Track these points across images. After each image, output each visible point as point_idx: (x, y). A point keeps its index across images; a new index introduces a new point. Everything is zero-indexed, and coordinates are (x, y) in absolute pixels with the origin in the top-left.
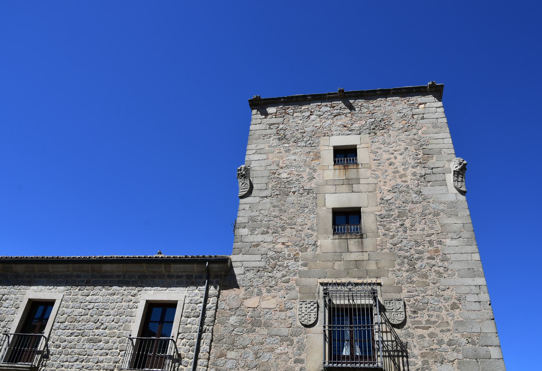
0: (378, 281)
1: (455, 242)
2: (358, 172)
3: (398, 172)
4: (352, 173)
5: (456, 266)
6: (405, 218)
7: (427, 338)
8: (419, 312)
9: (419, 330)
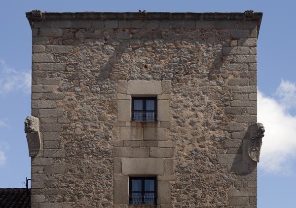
2: (156, 131)
4: (150, 131)
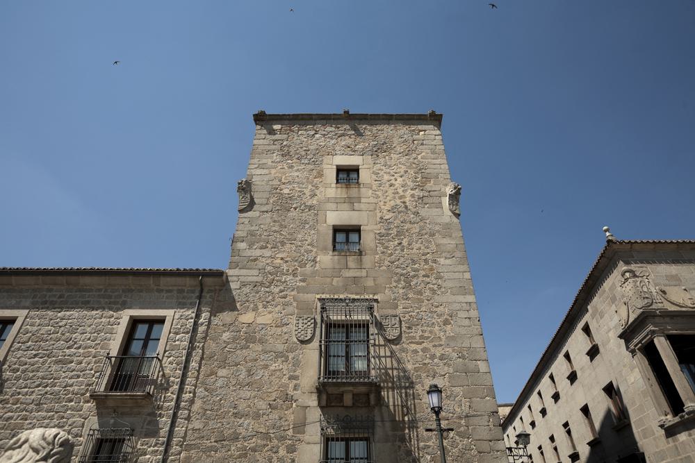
0: (376, 297)
1: (448, 262)
2: (359, 191)
3: (398, 193)
4: (354, 192)
5: (449, 284)
6: (403, 237)
7: (421, 353)
8: (413, 327)
9: (413, 345)
